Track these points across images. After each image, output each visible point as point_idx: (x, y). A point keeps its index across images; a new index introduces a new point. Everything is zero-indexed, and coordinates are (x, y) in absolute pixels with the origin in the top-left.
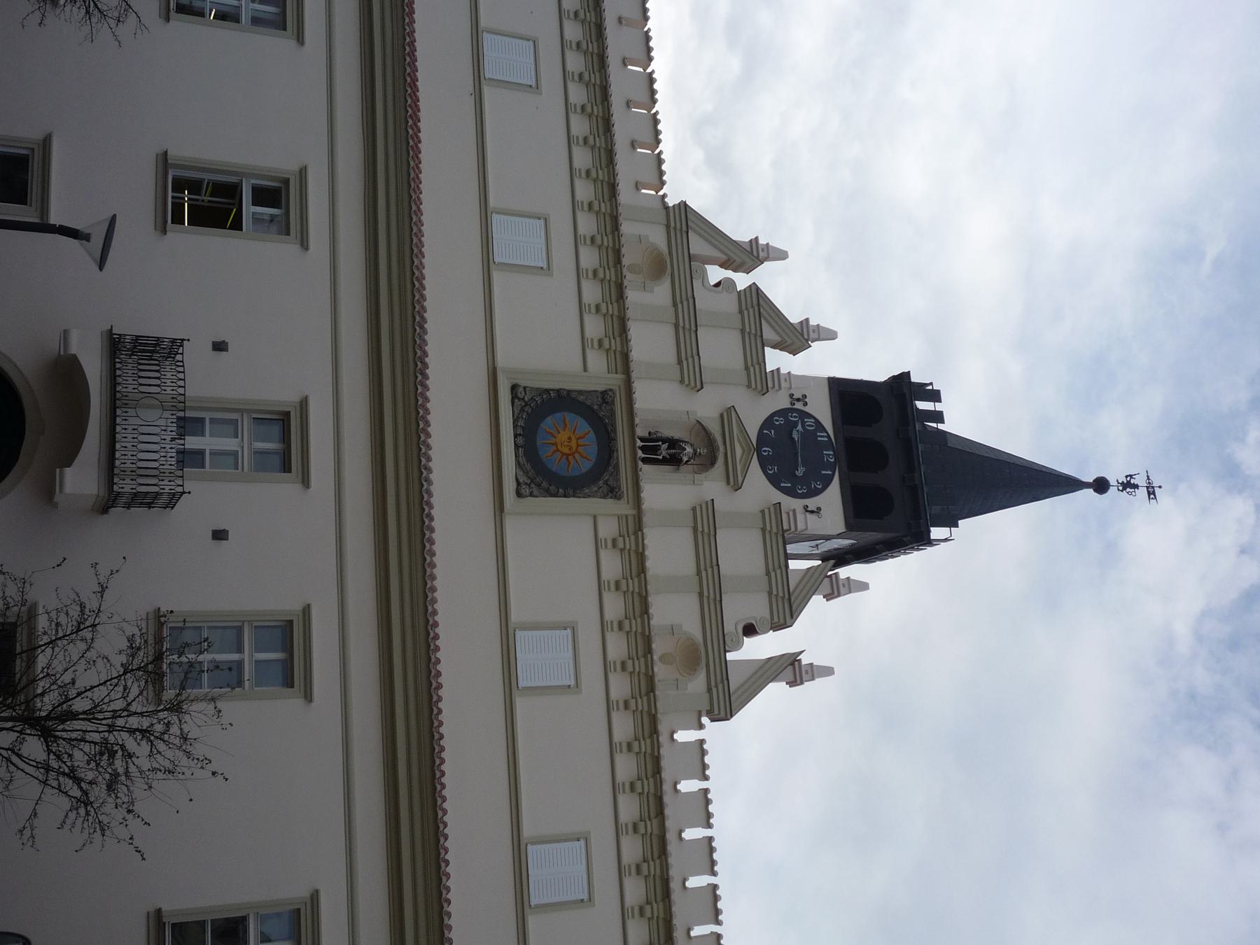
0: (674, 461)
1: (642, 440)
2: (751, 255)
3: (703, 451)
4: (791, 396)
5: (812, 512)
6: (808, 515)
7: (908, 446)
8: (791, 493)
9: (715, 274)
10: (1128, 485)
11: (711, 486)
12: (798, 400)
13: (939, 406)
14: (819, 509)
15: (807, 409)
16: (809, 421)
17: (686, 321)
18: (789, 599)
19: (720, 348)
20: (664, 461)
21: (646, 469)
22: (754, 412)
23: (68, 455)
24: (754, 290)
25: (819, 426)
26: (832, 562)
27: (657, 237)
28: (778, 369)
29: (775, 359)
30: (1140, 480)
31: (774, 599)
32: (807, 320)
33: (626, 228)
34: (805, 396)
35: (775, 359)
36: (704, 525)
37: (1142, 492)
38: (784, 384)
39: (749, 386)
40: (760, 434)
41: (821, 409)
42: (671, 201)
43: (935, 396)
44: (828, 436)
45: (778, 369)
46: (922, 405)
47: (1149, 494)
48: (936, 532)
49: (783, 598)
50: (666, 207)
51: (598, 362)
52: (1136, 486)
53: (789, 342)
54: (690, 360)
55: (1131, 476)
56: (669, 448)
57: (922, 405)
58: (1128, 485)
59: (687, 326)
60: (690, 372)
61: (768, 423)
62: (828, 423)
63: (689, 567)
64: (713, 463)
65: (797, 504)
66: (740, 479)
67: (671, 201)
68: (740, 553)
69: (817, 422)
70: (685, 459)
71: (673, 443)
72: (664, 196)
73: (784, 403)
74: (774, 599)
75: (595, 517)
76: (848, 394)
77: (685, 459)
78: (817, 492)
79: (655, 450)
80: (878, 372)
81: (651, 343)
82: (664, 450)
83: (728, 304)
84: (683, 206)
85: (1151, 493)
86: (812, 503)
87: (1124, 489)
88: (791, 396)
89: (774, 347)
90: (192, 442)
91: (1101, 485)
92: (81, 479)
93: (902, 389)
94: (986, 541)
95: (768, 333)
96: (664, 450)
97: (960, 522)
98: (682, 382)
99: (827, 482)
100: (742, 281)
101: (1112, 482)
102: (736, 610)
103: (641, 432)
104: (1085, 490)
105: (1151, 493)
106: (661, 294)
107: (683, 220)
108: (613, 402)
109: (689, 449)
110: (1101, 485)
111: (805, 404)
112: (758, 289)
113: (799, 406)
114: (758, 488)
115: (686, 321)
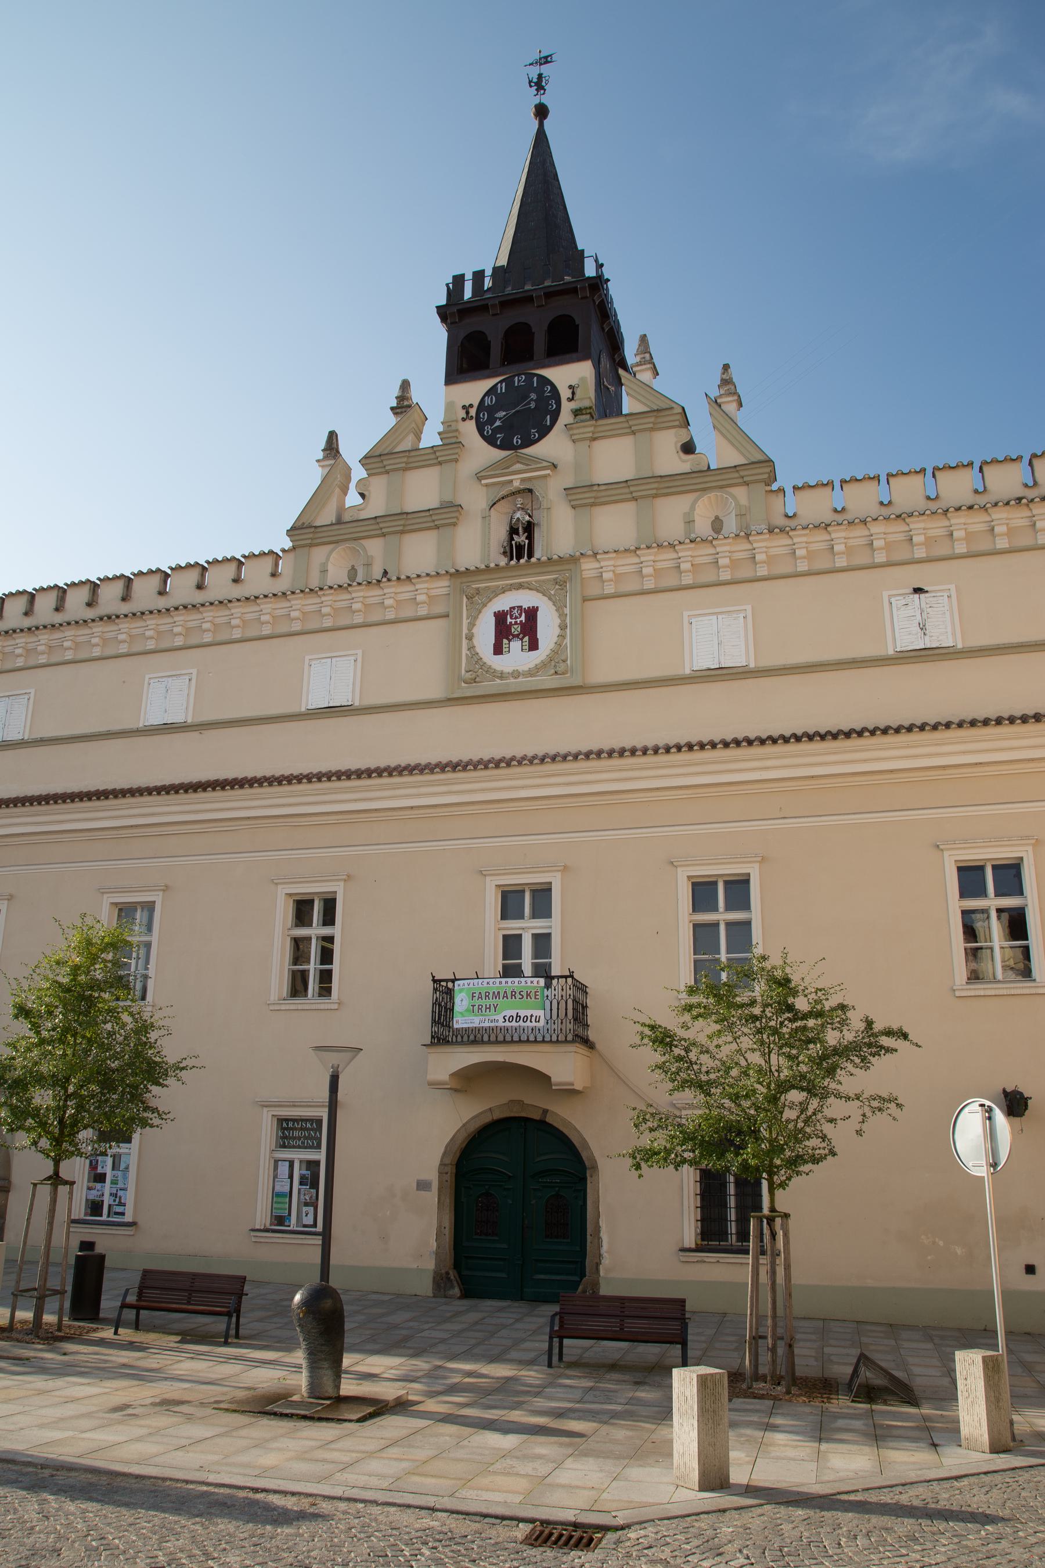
0: (529, 528)
1: (512, 559)
3: (519, 501)
4: (464, 420)
5: (573, 393)
6: (576, 397)
7: (507, 304)
8: (556, 415)
9: (353, 499)
10: (539, 85)
12: (467, 413)
13: (469, 276)
14: (570, 387)
15: (476, 404)
16: (487, 401)
17: (399, 523)
18: (658, 410)
19: (422, 490)
20: (530, 538)
21: (538, 553)
22: (480, 453)
23: (541, 1079)
24: (366, 460)
26: (621, 372)
27: (319, 554)
28: (439, 434)
29: (430, 438)
30: (534, 72)
31: (659, 426)
32: (392, 409)
33: (314, 583)
34: (464, 407)
35: (430, 438)
36: (587, 496)
37: (545, 69)
38: (453, 428)
39: (456, 461)
40: (501, 447)
41: (475, 391)
42: (288, 544)
43: (459, 280)
44: (501, 382)
45: (439, 434)
46: (468, 294)
47: (547, 62)
48: (590, 271)
49: (657, 417)
50: (294, 548)
52: (540, 76)
53: (413, 425)
54: (434, 518)
55: (530, 82)
56: (518, 534)
57: (468, 294)
58: (539, 85)
59: (402, 522)
60: (445, 516)
61: (490, 440)
62: (487, 384)
63: (630, 507)
64: (530, 491)
65: (566, 407)
66: (545, 464)
67: (288, 544)
69: (488, 393)
70: (527, 518)
71: (513, 531)
72: (283, 551)
73: (471, 425)
74: (659, 426)
75: (585, 600)
76: (463, 363)
77: (527, 518)
78: (554, 388)
79: (520, 547)
80: (439, 336)
82: (521, 539)
83: (379, 486)
84: (292, 532)
85: (546, 60)
86: (565, 393)
87: (543, 88)
88: (464, 420)
89: (419, 439)
90: (527, 969)
91: (542, 112)
92: (563, 1066)
93: (453, 312)
94: (596, 233)
95: (407, 444)
96: (521, 539)
97: (580, 248)
98: (454, 524)
99: (545, 381)
100: (358, 473)
101: (537, 102)
102: (668, 459)
103: (503, 561)
104: (546, 128)
105: (546, 60)
107: (303, 532)
108: (478, 589)
109: (518, 515)
110: (542, 112)
111: (471, 406)
112: (365, 457)
113: (473, 412)
114: (554, 446)
115: (399, 523)
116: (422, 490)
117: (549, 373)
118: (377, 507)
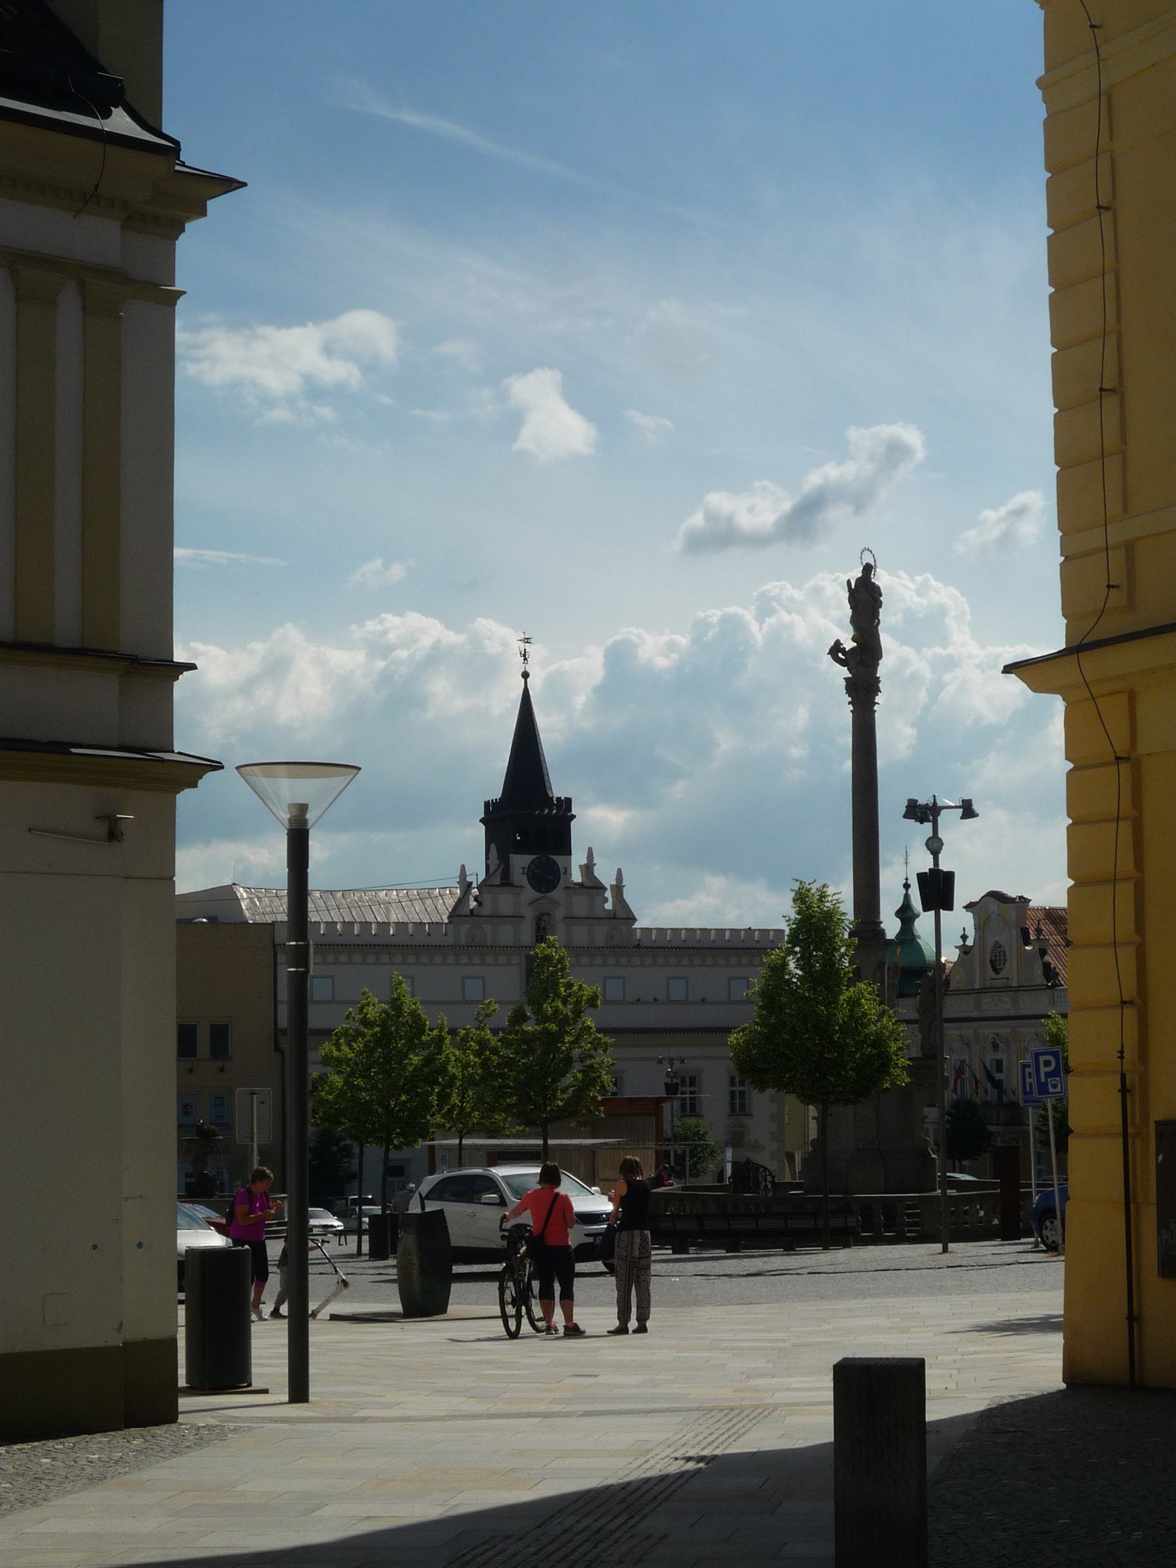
2: (466, 887)
10: (524, 655)
11: (559, 914)
17: (496, 918)
22: (529, 893)
25: (533, 862)
27: (465, 928)
51: (515, 960)
58: (524, 655)
62: (534, 857)
65: (562, 877)
68: (580, 905)
81: (505, 934)
83: (487, 899)
86: (562, 871)
91: (525, 675)
105: (527, 641)
106: (487, 928)
110: (525, 675)
114: (557, 894)
116: (506, 902)
117: (556, 858)
118: (487, 909)
